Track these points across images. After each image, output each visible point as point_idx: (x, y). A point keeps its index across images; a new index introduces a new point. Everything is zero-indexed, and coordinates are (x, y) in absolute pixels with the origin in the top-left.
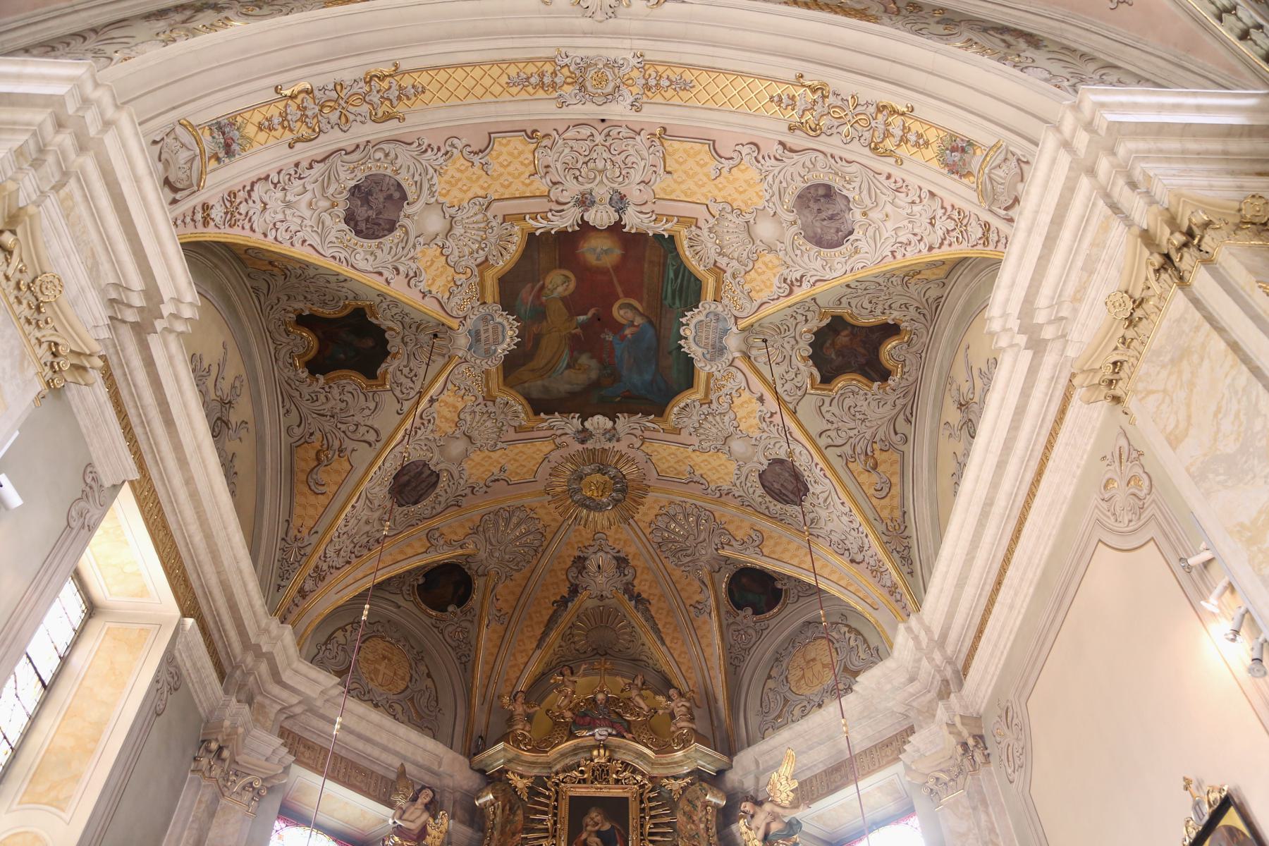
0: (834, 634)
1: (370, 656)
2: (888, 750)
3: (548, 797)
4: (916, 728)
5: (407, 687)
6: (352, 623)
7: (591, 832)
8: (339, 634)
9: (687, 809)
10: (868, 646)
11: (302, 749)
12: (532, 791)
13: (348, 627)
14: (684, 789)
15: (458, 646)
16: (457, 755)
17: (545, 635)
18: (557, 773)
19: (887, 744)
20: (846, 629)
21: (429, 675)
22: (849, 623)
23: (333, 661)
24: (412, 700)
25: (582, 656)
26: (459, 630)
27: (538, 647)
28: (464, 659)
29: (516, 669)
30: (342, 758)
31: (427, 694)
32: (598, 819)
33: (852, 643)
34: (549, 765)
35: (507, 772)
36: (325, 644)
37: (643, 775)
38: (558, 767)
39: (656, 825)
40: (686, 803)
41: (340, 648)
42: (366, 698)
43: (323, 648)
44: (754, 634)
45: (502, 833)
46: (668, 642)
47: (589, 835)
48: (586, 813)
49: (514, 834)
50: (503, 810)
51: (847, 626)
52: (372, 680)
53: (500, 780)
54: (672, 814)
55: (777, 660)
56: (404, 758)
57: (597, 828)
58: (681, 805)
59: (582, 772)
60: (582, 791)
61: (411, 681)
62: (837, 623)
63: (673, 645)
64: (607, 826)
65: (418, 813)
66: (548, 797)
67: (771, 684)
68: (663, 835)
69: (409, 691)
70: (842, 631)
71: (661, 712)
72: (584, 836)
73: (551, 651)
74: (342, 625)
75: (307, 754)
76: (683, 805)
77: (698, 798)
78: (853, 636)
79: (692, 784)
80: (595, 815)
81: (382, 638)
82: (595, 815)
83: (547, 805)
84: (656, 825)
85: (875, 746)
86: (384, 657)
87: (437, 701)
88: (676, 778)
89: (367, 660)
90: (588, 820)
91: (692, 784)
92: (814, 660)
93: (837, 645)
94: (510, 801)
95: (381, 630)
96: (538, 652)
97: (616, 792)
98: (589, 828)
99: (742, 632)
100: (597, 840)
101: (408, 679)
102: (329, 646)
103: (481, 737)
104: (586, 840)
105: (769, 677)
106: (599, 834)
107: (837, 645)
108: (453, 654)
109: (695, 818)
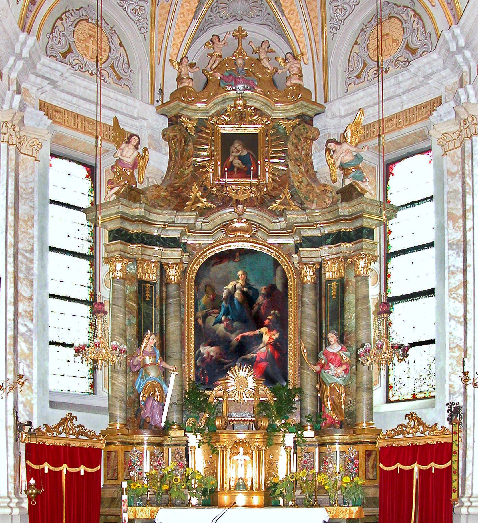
0: (404, 15)
1: (81, 37)
2: (424, 111)
3: (207, 134)
4: (443, 100)
5: (109, 56)
6: (65, 13)
7: (235, 156)
8: (59, 22)
9: (295, 141)
10: (425, 30)
11: (54, 113)
12: (198, 130)
13: (63, 17)
14: (294, 127)
15: (138, 20)
16: (147, 106)
17: (198, 8)
18: (212, 117)
19: (423, 106)
20: (413, 13)
21: (121, 45)
22: (415, 8)
23: (59, 45)
24: (112, 67)
25: (226, 21)
26: (138, 7)
27: (194, 18)
28: (143, 30)
29: (179, 36)
30: (78, 115)
31: (122, 60)
32: (239, 148)
33: (415, 26)
34: (207, 112)
35: (180, 117)
36: (52, 33)
37: (268, 117)
38: (213, 112)
39: (275, 152)
40: (294, 137)
41: (61, 34)
42: (84, 70)
43: (51, 36)
44: (348, 8)
45: (182, 158)
46: (286, 13)
47: (234, 158)
48: (232, 144)
49: (188, 158)
50: (180, 144)
51: (414, 10)
52: (85, 55)
53: (177, 123)
54: (285, 145)
55: (363, 30)
56: (116, 111)
57: (239, 154)
58: (291, 138)
59: (227, 116)
60: (228, 129)
61: (110, 51)
62: (408, 7)
63: (290, 16)
64: (245, 153)
65: (132, 151)
66: (207, 134)
67: (356, 49)
68: (279, 158)
69: (110, 59)
70: (410, 15)
71: (280, 72)
72: (231, 159)
73: (204, 20)
74: (59, 16)
75: (57, 116)
76: (292, 138)
77: (302, 135)
78: (416, 19)
79: (299, 124)
80: (237, 145)
81: (87, 20)
82: (237, 145)
83: (207, 139)
84: (275, 152)
85: (416, 107)
86: (90, 36)
87: (129, 64)
88: (289, 120)
89: (79, 40)
90: (233, 149)
91: (299, 124)
92: (387, 35)
93: (405, 25)
94: (184, 137)
95: (85, 14)
96: (195, 22)
97: (251, 129)
98: (234, 154)
99: (340, 7)
100: (239, 161)
101: (108, 50)
102: (54, 34)
103: (160, 89)
104: (232, 161)
105: (356, 43)
106: (240, 158)
107: (405, 25)
108: (135, 26)
109: (299, 148)
